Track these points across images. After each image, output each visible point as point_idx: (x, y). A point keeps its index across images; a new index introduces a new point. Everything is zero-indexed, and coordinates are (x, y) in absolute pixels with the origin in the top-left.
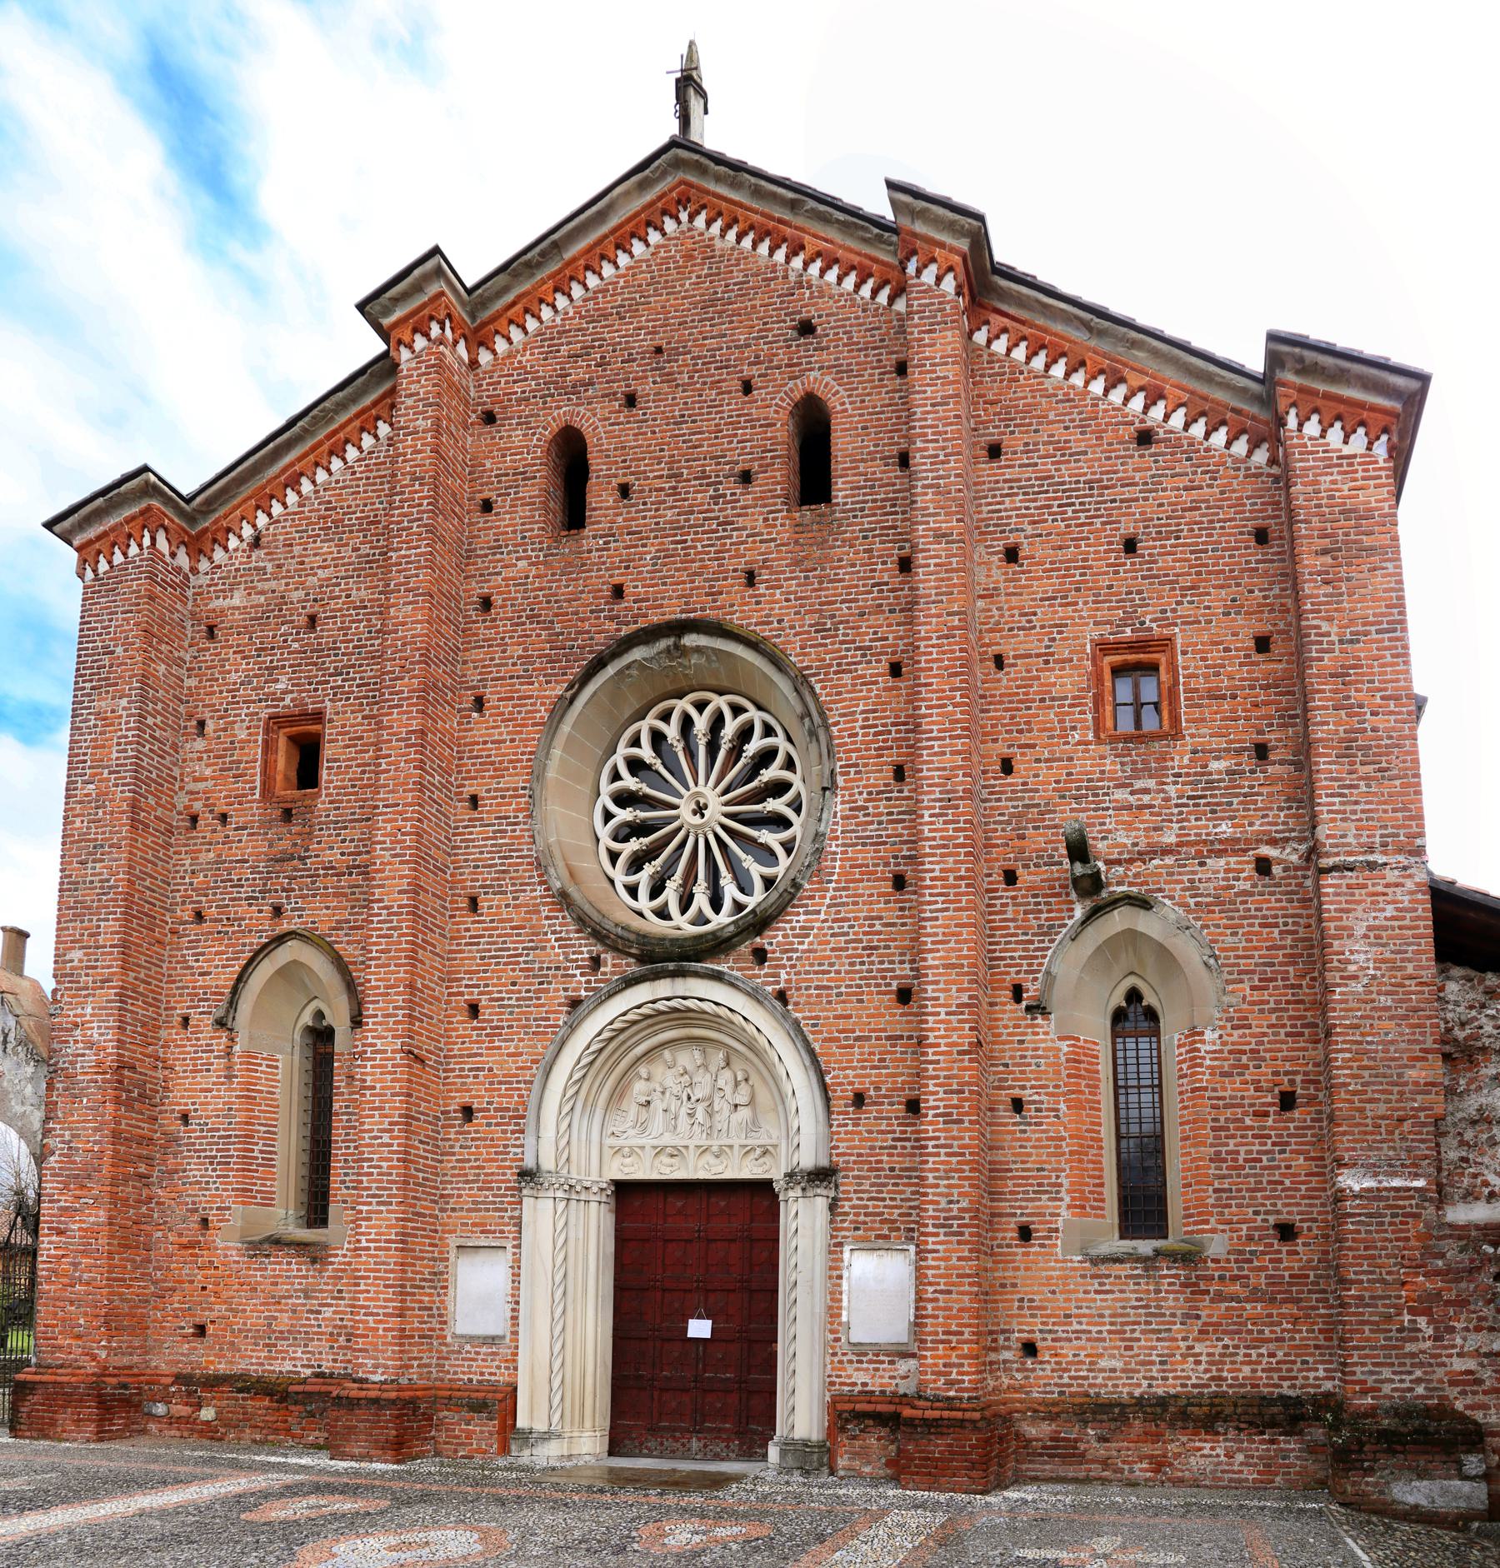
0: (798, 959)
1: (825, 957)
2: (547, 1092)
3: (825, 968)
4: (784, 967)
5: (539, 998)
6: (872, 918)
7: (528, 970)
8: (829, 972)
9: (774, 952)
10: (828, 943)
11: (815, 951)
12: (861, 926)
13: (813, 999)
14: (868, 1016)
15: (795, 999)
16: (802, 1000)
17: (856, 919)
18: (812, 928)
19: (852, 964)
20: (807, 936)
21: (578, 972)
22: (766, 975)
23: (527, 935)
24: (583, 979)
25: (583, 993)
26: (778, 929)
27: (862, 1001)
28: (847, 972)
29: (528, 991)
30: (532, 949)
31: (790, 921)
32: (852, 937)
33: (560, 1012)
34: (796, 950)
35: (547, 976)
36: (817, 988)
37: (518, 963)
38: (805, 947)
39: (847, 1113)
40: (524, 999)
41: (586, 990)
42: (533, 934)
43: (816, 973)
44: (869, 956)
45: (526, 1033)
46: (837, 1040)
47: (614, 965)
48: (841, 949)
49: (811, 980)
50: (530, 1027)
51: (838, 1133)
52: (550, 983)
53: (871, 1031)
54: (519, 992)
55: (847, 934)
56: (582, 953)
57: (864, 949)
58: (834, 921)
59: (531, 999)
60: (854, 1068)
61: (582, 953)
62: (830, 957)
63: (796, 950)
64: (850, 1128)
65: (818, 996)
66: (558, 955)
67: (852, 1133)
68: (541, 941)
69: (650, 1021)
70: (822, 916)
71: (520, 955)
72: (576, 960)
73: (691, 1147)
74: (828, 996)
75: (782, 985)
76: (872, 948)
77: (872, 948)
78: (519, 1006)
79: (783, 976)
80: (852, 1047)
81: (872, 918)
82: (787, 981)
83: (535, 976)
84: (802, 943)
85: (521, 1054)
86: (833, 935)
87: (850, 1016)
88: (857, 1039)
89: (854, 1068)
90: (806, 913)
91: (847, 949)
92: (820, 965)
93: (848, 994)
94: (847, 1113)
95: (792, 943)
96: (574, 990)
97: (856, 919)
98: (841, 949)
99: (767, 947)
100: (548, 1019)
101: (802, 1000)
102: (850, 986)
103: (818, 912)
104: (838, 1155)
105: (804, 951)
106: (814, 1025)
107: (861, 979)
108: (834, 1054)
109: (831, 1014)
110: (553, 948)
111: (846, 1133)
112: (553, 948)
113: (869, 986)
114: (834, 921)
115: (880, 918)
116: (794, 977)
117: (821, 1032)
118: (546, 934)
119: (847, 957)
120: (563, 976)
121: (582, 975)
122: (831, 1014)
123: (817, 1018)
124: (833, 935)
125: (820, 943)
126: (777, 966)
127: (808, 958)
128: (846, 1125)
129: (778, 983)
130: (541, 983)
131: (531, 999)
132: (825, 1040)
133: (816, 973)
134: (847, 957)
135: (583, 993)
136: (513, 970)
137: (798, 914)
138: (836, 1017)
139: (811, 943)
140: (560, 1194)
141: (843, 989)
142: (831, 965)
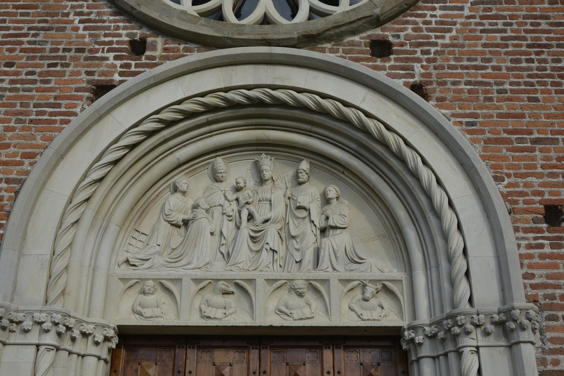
0: (436, 53)
1: (476, 53)
2: (45, 194)
3: (478, 63)
4: (419, 60)
5: (48, 82)
6: (535, 17)
7: (34, 50)
8: (485, 68)
9: (402, 45)
10: (480, 38)
11: (463, 46)
12: (519, 24)
13: (465, 95)
14: (548, 116)
15: (438, 94)
16: (449, 96)
17: (512, 17)
18: (455, 24)
19: (518, 61)
20: (450, 31)
21: (111, 55)
22: (392, 68)
23: (39, 15)
24: (118, 63)
25: (117, 77)
26: (407, 22)
27: (536, 100)
28: (508, 69)
29: (33, 73)
30: (43, 29)
31: (424, 16)
32: (509, 34)
33: (80, 98)
34: (436, 44)
35: (63, 58)
36: (468, 83)
37: (21, 43)
38: (447, 41)
39: (540, 231)
40: (23, 82)
41: (121, 74)
42: (47, 15)
43: (467, 68)
44: (537, 54)
45: (18, 121)
46: (508, 141)
47: (165, 50)
48: (498, 46)
49: (460, 75)
50: (27, 114)
51: (531, 256)
52: (68, 65)
53: (553, 133)
54: (17, 74)
55: (505, 31)
56: (120, 35)
57: (529, 46)
58: (482, 18)
59: (34, 82)
60: (541, 176)
61: (120, 35)
62: (483, 53)
63: (436, 44)
64: (547, 250)
65: (470, 92)
66: (84, 36)
67: (551, 256)
68: (58, 22)
69: (210, 116)
70: (466, 12)
71: (26, 35)
72: (111, 43)
73: (260, 282)
74: (486, 92)
75: (417, 79)
76: (540, 46)
77: (540, 46)
78: (11, 90)
79: (418, 68)
80: (532, 150)
81: (535, 17)
82: (423, 75)
83: (42, 58)
84: (443, 37)
85: (7, 146)
86: (482, 31)
87: (523, 116)
88: (536, 141)
89: (541, 176)
90: (441, 8)
91: (507, 46)
92: (469, 60)
93: (512, 91)
94: (540, 231)
95: (429, 37)
96: (103, 74)
97: (512, 17)
98: (498, 46)
99: (391, 39)
100: (59, 106)
101: (449, 96)
102: (518, 84)
103: (462, 9)
104: (533, 287)
105: (443, 45)
106: (468, 124)
107: (530, 76)
108: (505, 158)
109: (495, 112)
110: (76, 29)
111: (543, 256)
112: (77, 29)
113: (545, 84)
114: (482, 18)
115: (547, 18)
116: (434, 72)
117: (482, 132)
118: (67, 15)
119: (507, 53)
120: (86, 59)
121: (116, 58)
122: (495, 112)
123: (476, 116)
124: (482, 31)
125: (466, 38)
126: (407, 60)
127: (453, 53)
128: (541, 246)
129: (413, 76)
130: (55, 65)
131: (34, 82)
132: (488, 141)
133: (467, 68)
134: (507, 53)
135: (117, 77)
136: (11, 50)
137: (434, 9)
138: (500, 116)
139: (455, 38)
140: (50, 339)
141: (507, 87)
142: (489, 60)
